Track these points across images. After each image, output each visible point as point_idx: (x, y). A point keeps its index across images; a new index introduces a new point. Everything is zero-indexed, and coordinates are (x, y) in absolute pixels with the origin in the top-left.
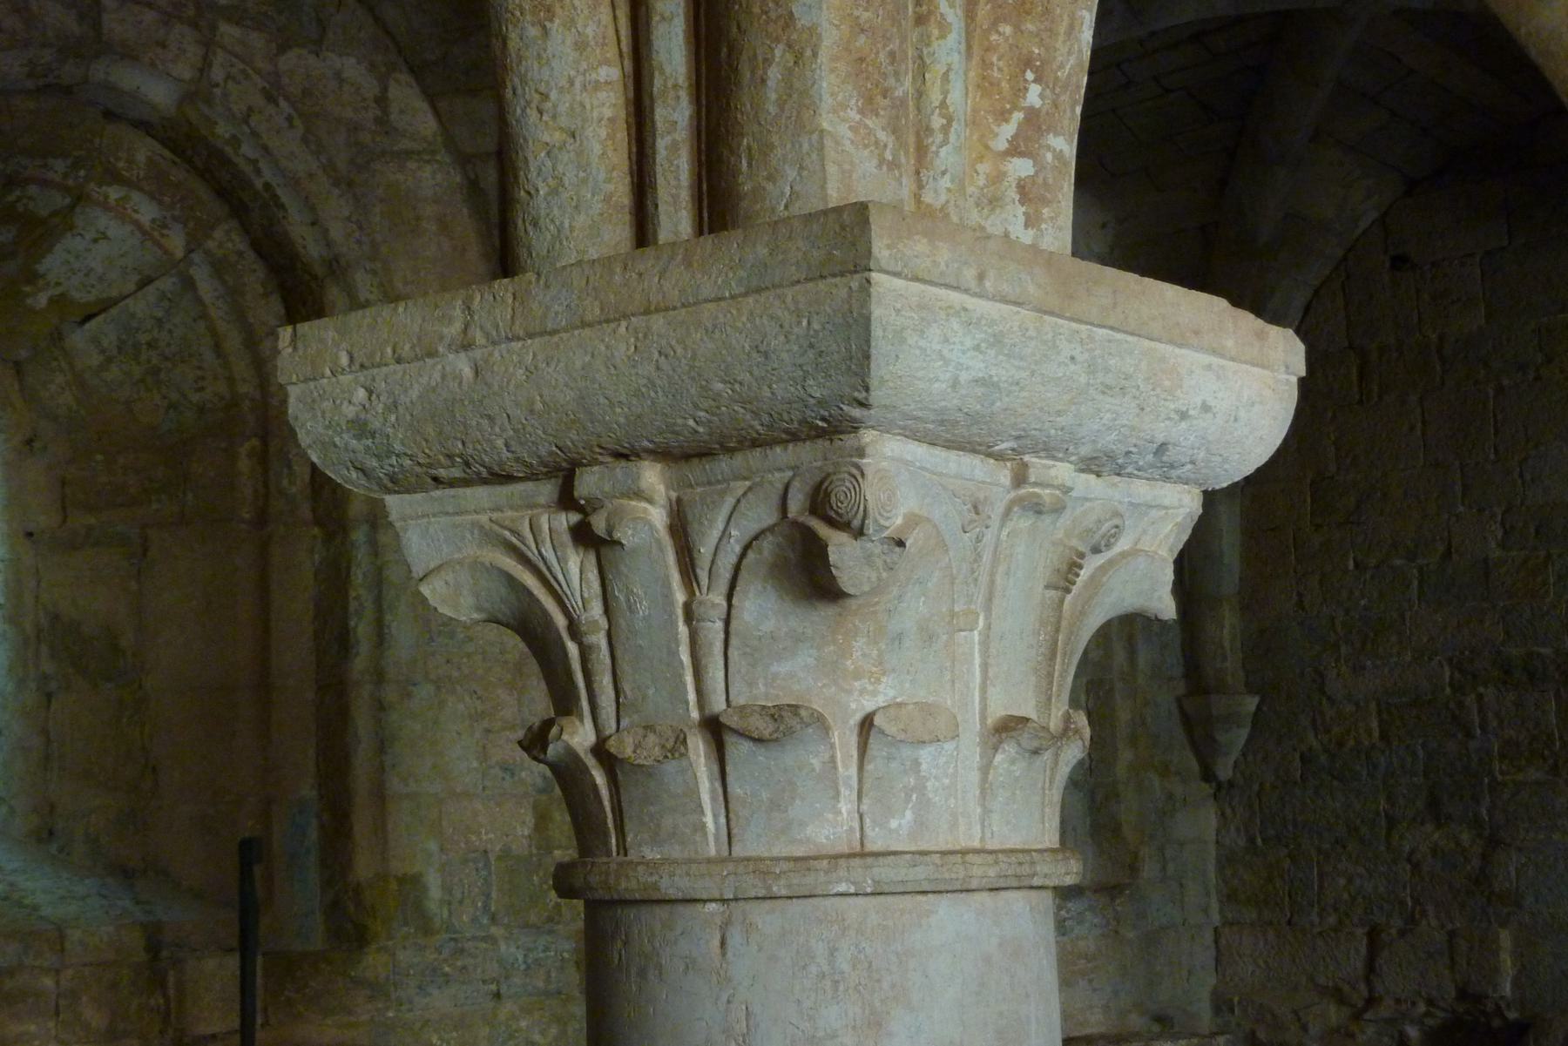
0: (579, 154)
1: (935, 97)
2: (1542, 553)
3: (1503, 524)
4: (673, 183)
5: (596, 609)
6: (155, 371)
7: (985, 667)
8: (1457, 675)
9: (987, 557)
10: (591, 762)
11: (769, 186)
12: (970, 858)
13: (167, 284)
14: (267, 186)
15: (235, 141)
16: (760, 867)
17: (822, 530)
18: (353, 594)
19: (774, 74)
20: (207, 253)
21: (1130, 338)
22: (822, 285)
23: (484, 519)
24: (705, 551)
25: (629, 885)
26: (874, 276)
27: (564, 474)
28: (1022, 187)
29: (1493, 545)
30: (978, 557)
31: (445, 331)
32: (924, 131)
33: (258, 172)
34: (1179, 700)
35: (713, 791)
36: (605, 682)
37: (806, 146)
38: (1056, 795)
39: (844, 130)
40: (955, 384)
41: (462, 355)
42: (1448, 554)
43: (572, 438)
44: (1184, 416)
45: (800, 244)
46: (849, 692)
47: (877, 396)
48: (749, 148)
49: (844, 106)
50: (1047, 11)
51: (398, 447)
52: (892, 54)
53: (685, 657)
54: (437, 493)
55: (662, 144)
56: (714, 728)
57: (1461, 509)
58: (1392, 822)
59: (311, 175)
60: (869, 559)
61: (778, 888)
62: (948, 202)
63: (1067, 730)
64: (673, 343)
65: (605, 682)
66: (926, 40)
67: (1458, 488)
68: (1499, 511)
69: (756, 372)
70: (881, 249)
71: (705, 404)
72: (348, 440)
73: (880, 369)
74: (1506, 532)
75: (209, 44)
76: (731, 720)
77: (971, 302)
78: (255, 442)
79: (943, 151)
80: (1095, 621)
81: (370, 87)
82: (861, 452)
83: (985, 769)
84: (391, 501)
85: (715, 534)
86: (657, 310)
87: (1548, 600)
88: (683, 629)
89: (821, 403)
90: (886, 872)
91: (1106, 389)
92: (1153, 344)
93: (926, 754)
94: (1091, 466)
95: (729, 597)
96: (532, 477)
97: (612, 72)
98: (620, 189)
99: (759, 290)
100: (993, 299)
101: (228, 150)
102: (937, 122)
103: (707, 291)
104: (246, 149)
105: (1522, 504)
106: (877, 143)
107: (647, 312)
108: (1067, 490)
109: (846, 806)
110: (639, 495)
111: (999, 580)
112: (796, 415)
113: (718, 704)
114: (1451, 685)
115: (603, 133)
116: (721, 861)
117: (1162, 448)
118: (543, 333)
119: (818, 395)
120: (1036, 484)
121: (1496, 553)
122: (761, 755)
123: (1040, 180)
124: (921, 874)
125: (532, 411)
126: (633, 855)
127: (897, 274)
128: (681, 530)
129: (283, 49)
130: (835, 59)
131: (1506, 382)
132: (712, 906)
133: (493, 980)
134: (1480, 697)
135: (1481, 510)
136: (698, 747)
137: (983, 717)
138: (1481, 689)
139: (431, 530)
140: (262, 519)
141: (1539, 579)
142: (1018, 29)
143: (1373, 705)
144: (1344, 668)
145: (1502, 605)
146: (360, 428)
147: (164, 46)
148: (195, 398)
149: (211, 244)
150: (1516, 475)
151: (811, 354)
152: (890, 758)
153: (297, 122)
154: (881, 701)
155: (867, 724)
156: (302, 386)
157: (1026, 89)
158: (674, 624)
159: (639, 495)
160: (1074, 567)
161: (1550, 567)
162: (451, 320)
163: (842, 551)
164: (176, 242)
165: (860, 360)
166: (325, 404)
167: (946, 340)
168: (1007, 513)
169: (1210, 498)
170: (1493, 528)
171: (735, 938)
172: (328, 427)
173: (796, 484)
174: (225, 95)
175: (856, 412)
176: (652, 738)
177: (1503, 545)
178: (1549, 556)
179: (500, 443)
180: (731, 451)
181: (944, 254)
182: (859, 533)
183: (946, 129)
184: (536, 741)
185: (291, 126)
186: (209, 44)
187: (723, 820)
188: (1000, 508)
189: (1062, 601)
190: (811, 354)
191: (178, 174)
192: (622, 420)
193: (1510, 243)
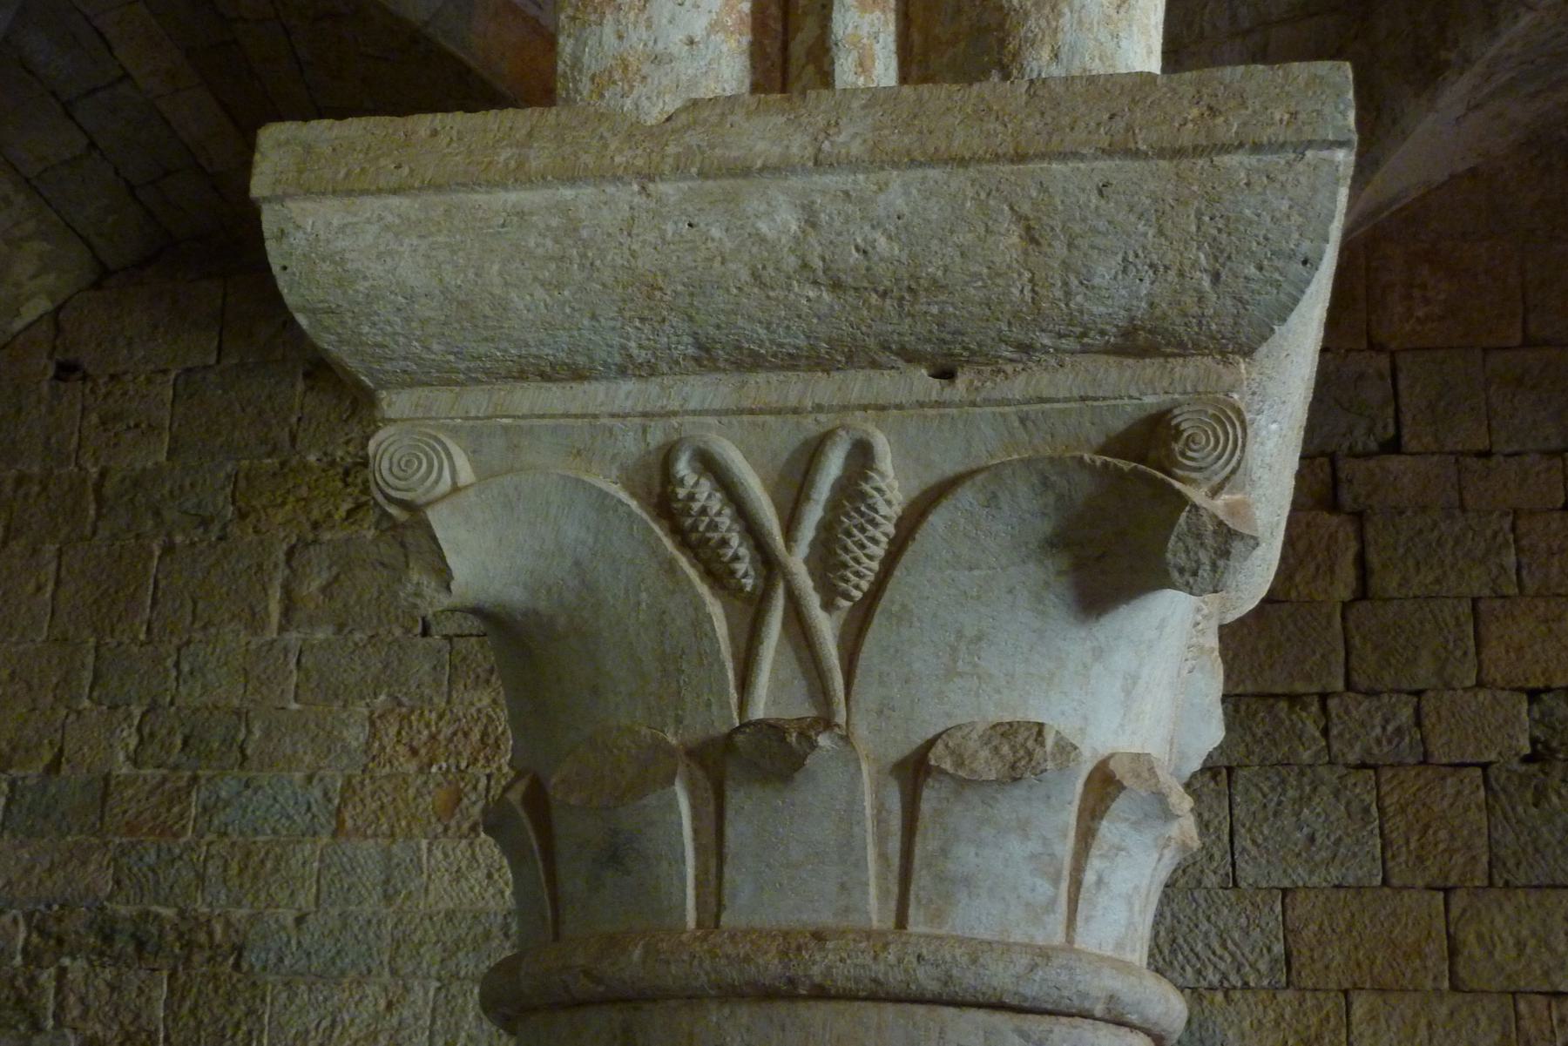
2: (188, 774)
3: (139, 730)
8: (35, 938)
29: (121, 757)
42: (54, 767)
57: (86, 703)
67: (87, 676)
68: (137, 712)
74: (141, 741)
87: (182, 840)
105: (172, 703)
114: (25, 952)
121: (124, 769)
131: (179, 539)
134: (63, 971)
135: (114, 707)
138: (66, 961)
141: (176, 810)
145: (117, 841)
150: (169, 663)
161: (194, 794)
170: (125, 734)
177: (135, 760)
178: (195, 779)
193: (218, 361)
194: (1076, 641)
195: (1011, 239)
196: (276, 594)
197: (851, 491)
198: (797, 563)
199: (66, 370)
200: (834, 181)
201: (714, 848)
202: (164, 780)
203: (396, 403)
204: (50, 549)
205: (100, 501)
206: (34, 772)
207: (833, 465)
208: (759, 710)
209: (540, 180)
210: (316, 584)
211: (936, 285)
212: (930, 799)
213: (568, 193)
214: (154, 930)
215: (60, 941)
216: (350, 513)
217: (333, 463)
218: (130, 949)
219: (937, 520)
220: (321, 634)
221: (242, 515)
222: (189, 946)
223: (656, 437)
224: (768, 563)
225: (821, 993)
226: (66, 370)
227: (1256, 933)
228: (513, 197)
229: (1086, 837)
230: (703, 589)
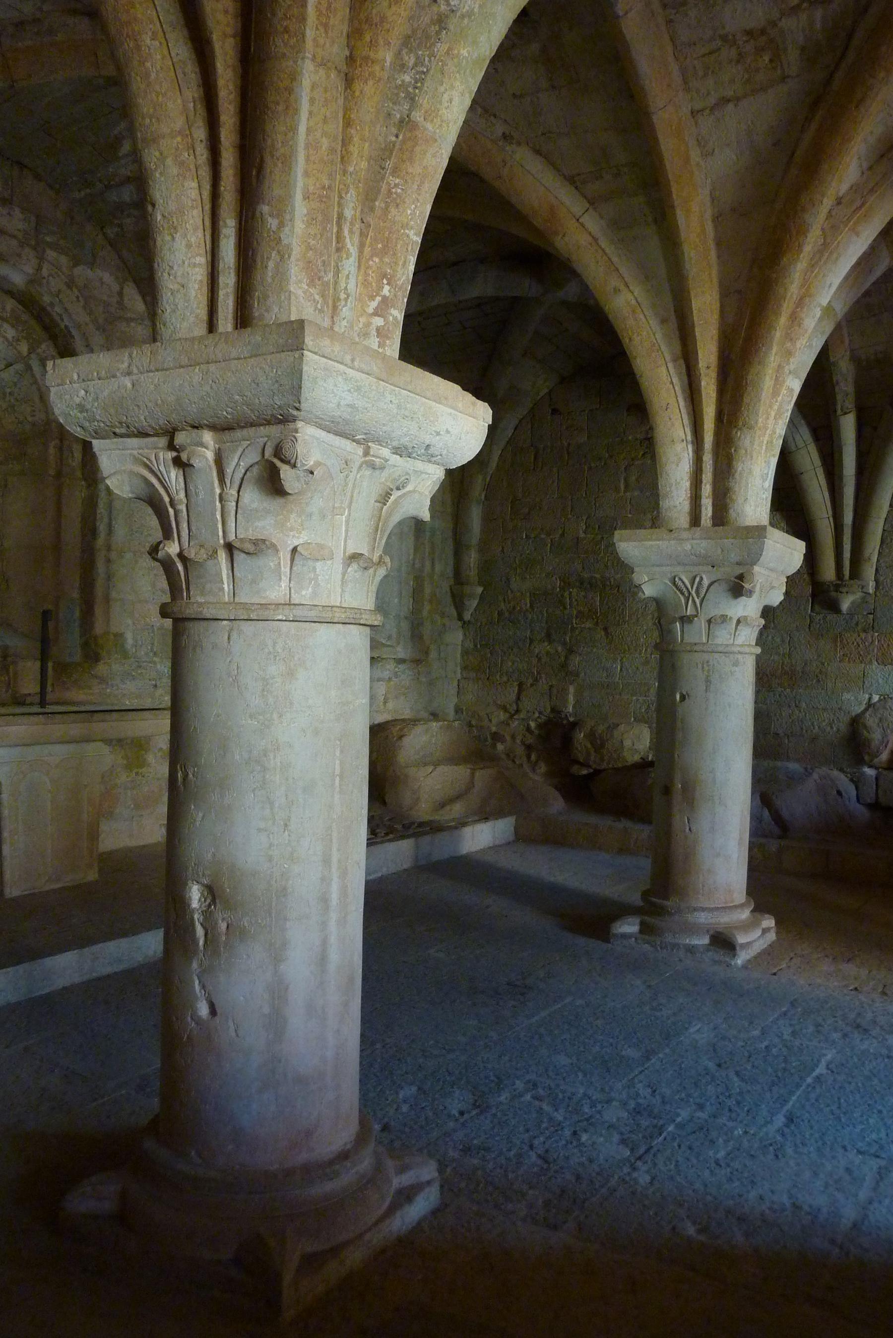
0: (185, 295)
1: (343, 285)
2: (600, 537)
4: (225, 311)
5: (182, 495)
6: (13, 406)
7: (347, 531)
9: (350, 485)
10: (177, 560)
11: (266, 314)
12: (334, 609)
13: (19, 367)
14: (66, 327)
15: (52, 304)
16: (245, 606)
17: (278, 463)
18: (98, 512)
19: (271, 265)
20: (38, 354)
21: (417, 397)
22: (283, 355)
23: (135, 452)
24: (229, 471)
25: (190, 612)
26: (305, 352)
27: (170, 433)
28: (378, 330)
29: (581, 532)
30: (346, 485)
31: (120, 366)
32: (336, 299)
33: (62, 320)
34: (451, 586)
35: (228, 574)
36: (185, 525)
37: (283, 297)
38: (374, 588)
39: (300, 293)
40: (339, 405)
41: (127, 378)
42: (563, 535)
43: (174, 418)
44: (438, 434)
45: (275, 336)
46: (288, 536)
47: (303, 406)
48: (259, 297)
49: (300, 282)
50: (394, 254)
51: (98, 417)
52: (324, 262)
53: (219, 517)
54: (115, 440)
55: (221, 293)
56: (230, 548)
57: (570, 516)
58: (531, 641)
59: (86, 324)
60: (298, 478)
61: (253, 616)
62: (345, 331)
63: (381, 562)
64: (218, 377)
65: (185, 525)
66: (340, 259)
67: (569, 510)
68: (585, 518)
69: (253, 393)
70: (309, 340)
71: (232, 405)
72: (75, 412)
73: (305, 394)
75: (41, 258)
76: (237, 544)
77: (349, 371)
78: (57, 441)
79: (344, 309)
80: (396, 518)
81: (116, 287)
82: (296, 431)
83: (344, 574)
84: (96, 443)
85: (234, 464)
86: (212, 362)
88: (218, 504)
89: (280, 407)
90: (299, 613)
91: (405, 417)
92: (427, 401)
93: (319, 565)
94: (398, 451)
95: (239, 492)
96: (156, 435)
97: (202, 260)
98: (203, 312)
99: (256, 356)
100: (358, 370)
101: (49, 308)
102: (343, 296)
103: (234, 354)
104: (58, 309)
106: (314, 300)
107: (208, 363)
108: (387, 461)
109: (284, 584)
110: (202, 445)
111: (355, 495)
112: (269, 412)
113: (231, 537)
114: (560, 587)
115: (197, 286)
116: (229, 603)
117: (428, 447)
118: (163, 370)
119: (279, 404)
120: (373, 456)
121: (582, 535)
122: (249, 560)
123: (386, 328)
124: (313, 614)
125: (157, 405)
126: (192, 600)
127: (315, 353)
128: (219, 461)
129: (76, 265)
130: (298, 260)
131: (593, 465)
132: (225, 622)
133: (154, 679)
134: (571, 593)
135: (578, 517)
136: (222, 555)
137: (345, 552)
139: (112, 456)
140: (59, 475)
142: (381, 260)
143: (528, 594)
144: (518, 578)
146: (81, 408)
147: (19, 255)
148: (30, 419)
149: (39, 350)
150: (593, 504)
151: (276, 385)
152: (303, 565)
153: (81, 299)
154: (301, 541)
155: (294, 550)
156: (57, 388)
157: (383, 287)
158: (214, 502)
159: (202, 445)
160: (388, 494)
162: (123, 362)
163: (286, 472)
164: (24, 348)
165: (297, 389)
166: (66, 396)
167: (336, 386)
168: (361, 466)
169: (449, 473)
171: (234, 635)
172: (67, 407)
173: (269, 443)
174: (48, 282)
175: (295, 413)
176: (203, 551)
178: (602, 538)
179: (142, 418)
180: (243, 427)
181: (337, 348)
182: (294, 466)
183: (346, 300)
184: (154, 551)
185: (78, 300)
186: (41, 258)
187: (231, 587)
188: (357, 464)
189: (382, 508)
190: (276, 385)
191: (25, 317)
192: (195, 410)
194: (734, 602)
195: (719, 551)
196: (622, 481)
197: (700, 583)
198: (693, 593)
199: (555, 411)
200: (695, 541)
201: (682, 631)
202: (593, 539)
203: (636, 569)
204: (555, 470)
205: (568, 453)
206: (557, 536)
207: (697, 579)
208: (688, 613)
210: (634, 478)
211: (709, 557)
214: (594, 581)
215: (569, 584)
216: (643, 455)
217: (637, 439)
218: (588, 586)
220: (636, 493)
221: (611, 457)
222: (604, 586)
223: (673, 575)
224: (690, 593)
226: (555, 411)
229: (736, 629)
230: (680, 595)
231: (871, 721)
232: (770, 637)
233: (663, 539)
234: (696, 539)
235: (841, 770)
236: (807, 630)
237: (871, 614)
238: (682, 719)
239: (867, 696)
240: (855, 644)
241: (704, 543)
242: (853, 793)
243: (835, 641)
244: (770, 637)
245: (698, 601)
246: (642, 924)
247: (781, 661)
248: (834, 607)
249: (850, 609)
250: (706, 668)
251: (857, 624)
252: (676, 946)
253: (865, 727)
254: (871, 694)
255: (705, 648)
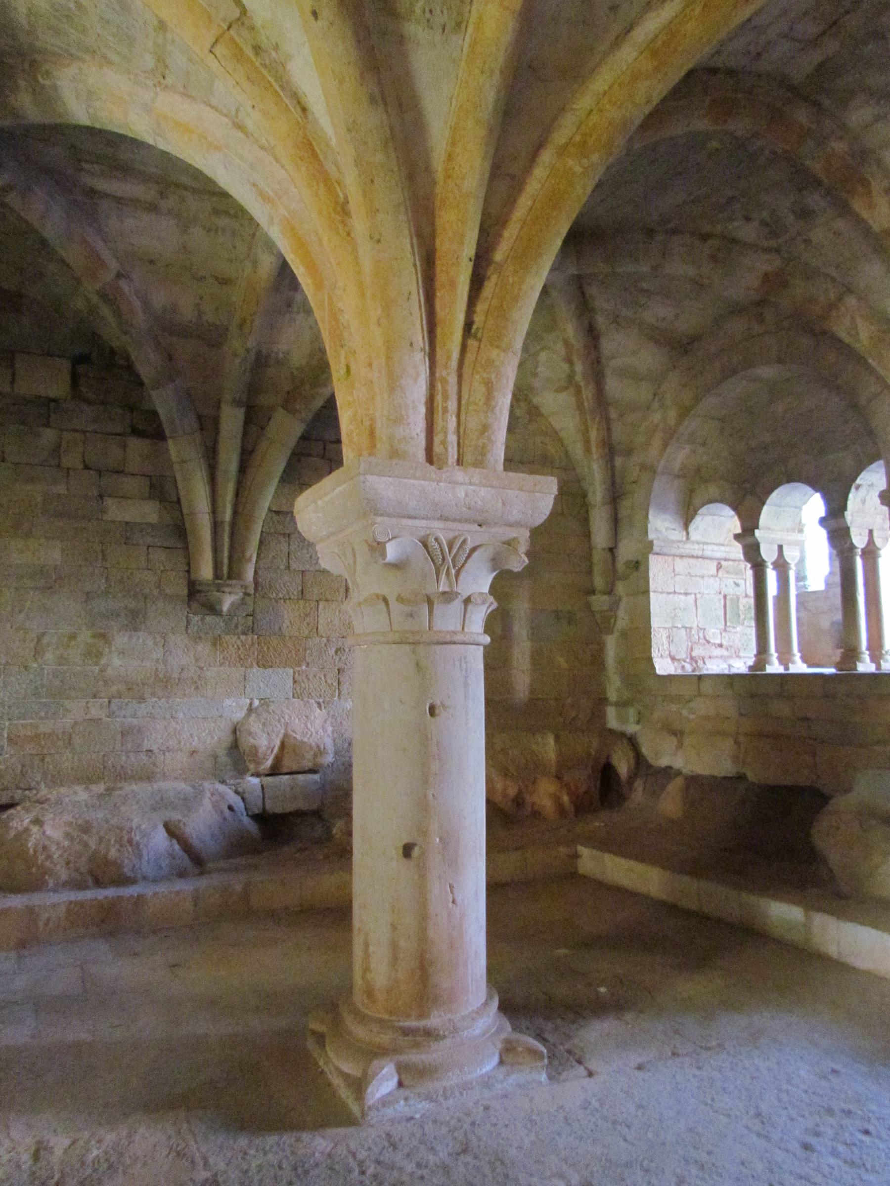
195: (500, 505)
200: (472, 488)
209: (416, 479)
211: (487, 511)
212: (470, 607)
213: (423, 482)
219: (476, 554)
223: (428, 532)
225: (455, 643)
227: (294, 584)
228: (412, 481)
231: (255, 725)
232: (141, 640)
233: (431, 480)
234: (474, 485)
235: (223, 782)
236: (184, 632)
237: (250, 615)
238: (438, 742)
239: (248, 701)
240: (236, 647)
241: (483, 492)
242: (242, 805)
243: (214, 645)
244: (141, 640)
245: (453, 571)
246: (401, 1069)
247: (154, 668)
248: (212, 609)
249: (229, 610)
250: (464, 666)
251: (236, 626)
252: (466, 1087)
253: (250, 734)
254: (251, 699)
255: (458, 638)
